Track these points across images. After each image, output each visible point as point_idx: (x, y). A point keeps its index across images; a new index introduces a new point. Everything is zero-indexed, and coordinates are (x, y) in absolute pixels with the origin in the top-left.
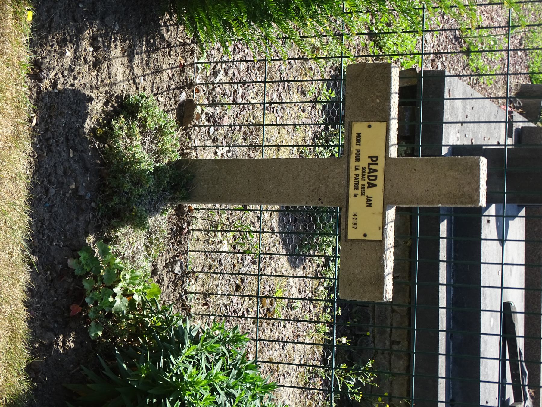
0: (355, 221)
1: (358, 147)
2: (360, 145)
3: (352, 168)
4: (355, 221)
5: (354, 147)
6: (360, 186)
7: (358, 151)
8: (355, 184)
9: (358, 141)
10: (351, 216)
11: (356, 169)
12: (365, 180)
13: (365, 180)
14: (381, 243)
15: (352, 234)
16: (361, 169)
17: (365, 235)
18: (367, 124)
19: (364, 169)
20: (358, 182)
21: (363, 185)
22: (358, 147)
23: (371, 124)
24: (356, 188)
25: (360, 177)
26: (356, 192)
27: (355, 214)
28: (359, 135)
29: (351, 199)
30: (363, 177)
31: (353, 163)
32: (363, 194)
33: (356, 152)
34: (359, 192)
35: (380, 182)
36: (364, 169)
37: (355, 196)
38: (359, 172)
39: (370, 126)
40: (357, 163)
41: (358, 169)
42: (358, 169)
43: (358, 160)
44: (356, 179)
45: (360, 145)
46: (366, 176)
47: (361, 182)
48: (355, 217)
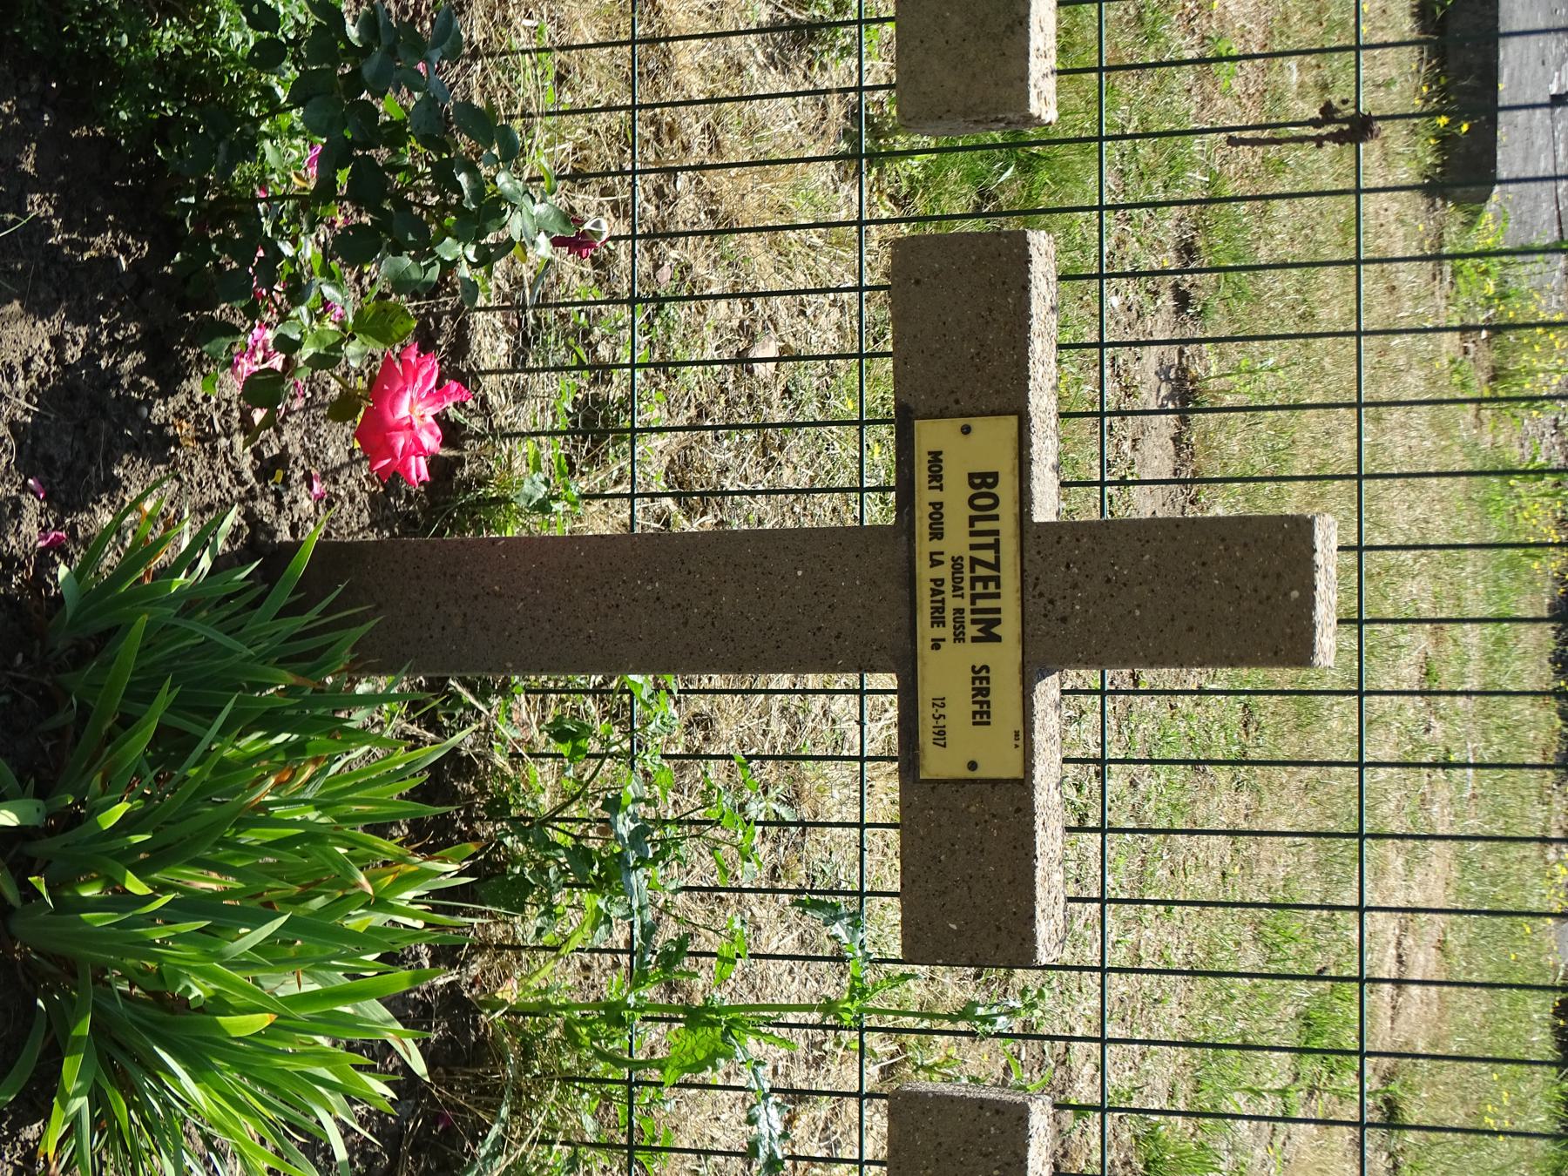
1: (935, 496)
2: (941, 488)
4: (941, 722)
5: (924, 496)
6: (949, 616)
7: (937, 506)
8: (935, 610)
9: (936, 477)
10: (926, 712)
11: (935, 563)
12: (962, 596)
13: (962, 596)
14: (1024, 784)
15: (938, 763)
16: (948, 564)
17: (973, 766)
19: (957, 562)
20: (943, 601)
21: (959, 611)
22: (935, 496)
23: (975, 422)
24: (938, 621)
25: (948, 587)
26: (938, 632)
27: (939, 703)
28: (936, 457)
30: (957, 588)
31: (924, 546)
32: (959, 637)
33: (931, 509)
34: (947, 632)
36: (957, 562)
37: (936, 644)
38: (945, 572)
39: (966, 430)
40: (936, 545)
41: (941, 563)
42: (941, 563)
43: (937, 534)
44: (935, 592)
45: (941, 488)
46: (967, 591)
47: (951, 603)
48: (941, 711)
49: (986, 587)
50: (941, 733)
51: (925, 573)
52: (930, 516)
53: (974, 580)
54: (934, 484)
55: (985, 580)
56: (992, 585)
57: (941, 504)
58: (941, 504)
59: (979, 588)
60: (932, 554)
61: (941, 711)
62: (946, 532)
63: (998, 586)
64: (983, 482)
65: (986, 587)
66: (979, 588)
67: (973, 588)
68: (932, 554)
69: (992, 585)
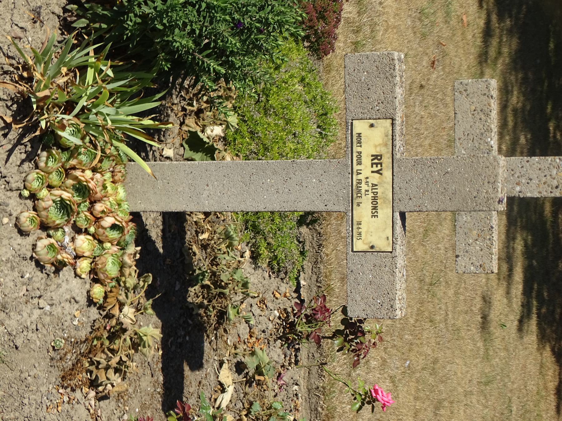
1: (359, 149)
2: (361, 146)
4: (360, 230)
5: (356, 149)
9: (359, 142)
10: (355, 227)
17: (372, 247)
27: (359, 223)
28: (359, 135)
31: (356, 167)
39: (372, 126)
40: (359, 167)
43: (359, 163)
45: (361, 146)
48: (360, 226)
49: (377, 167)
50: (360, 234)
53: (372, 164)
54: (359, 145)
55: (377, 164)
56: (379, 166)
59: (374, 166)
60: (357, 170)
61: (360, 226)
62: (362, 162)
63: (381, 166)
65: (377, 167)
66: (374, 166)
67: (372, 167)
69: (379, 166)
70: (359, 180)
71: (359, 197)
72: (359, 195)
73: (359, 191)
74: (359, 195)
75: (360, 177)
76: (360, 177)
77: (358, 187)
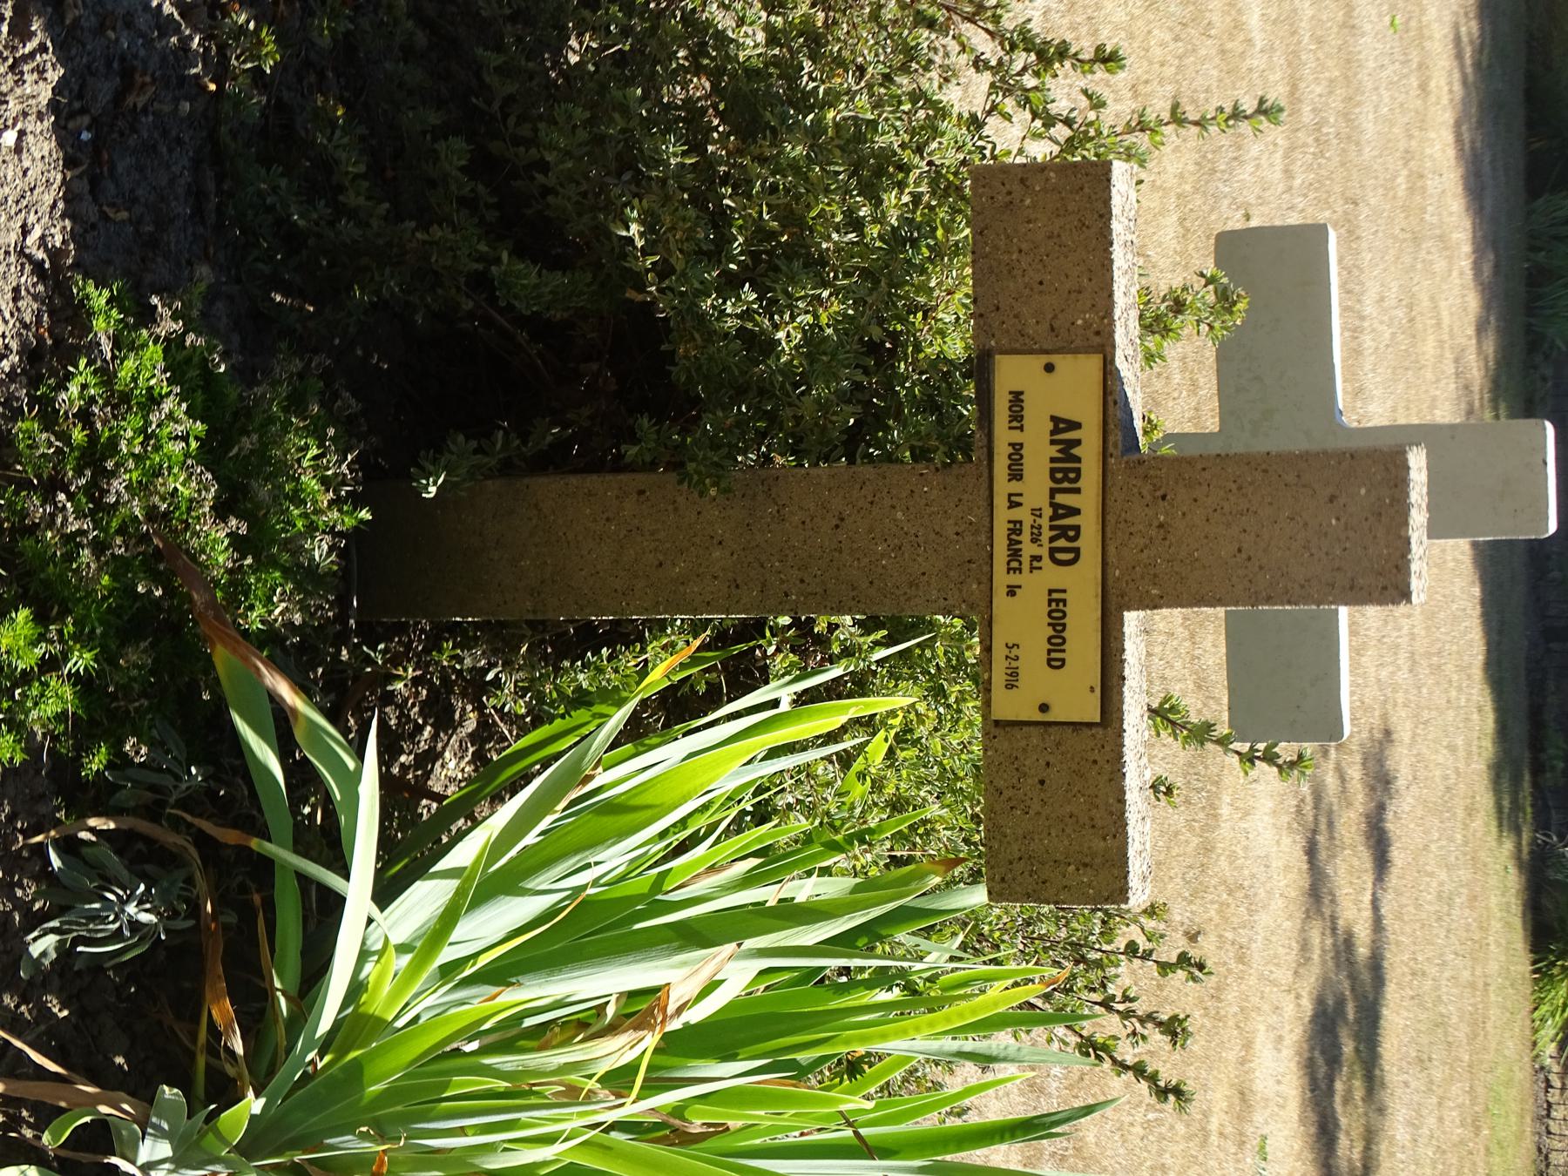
0: (1014, 664)
1: (1016, 437)
2: (1021, 428)
3: (1000, 501)
4: (1014, 664)
5: (1003, 436)
6: (1026, 560)
7: (1017, 447)
9: (1017, 417)
10: (999, 652)
15: (1009, 706)
18: (1045, 359)
22: (1016, 437)
23: (1055, 359)
28: (1017, 398)
29: (1000, 598)
31: (1003, 486)
33: (1011, 450)
35: (1089, 541)
39: (1049, 368)
40: (1015, 487)
41: (1020, 504)
42: (1020, 504)
43: (1016, 475)
45: (1021, 428)
51: (1002, 515)
52: (1010, 457)
54: (1015, 424)
57: (1021, 445)
58: (1021, 445)
60: (1010, 495)
62: (1025, 473)
64: (1061, 425)
68: (1010, 495)
70: (1015, 522)
71: (1015, 570)
72: (1014, 564)
73: (1015, 554)
74: (1014, 564)
75: (1016, 514)
76: (1016, 514)
77: (1012, 542)
